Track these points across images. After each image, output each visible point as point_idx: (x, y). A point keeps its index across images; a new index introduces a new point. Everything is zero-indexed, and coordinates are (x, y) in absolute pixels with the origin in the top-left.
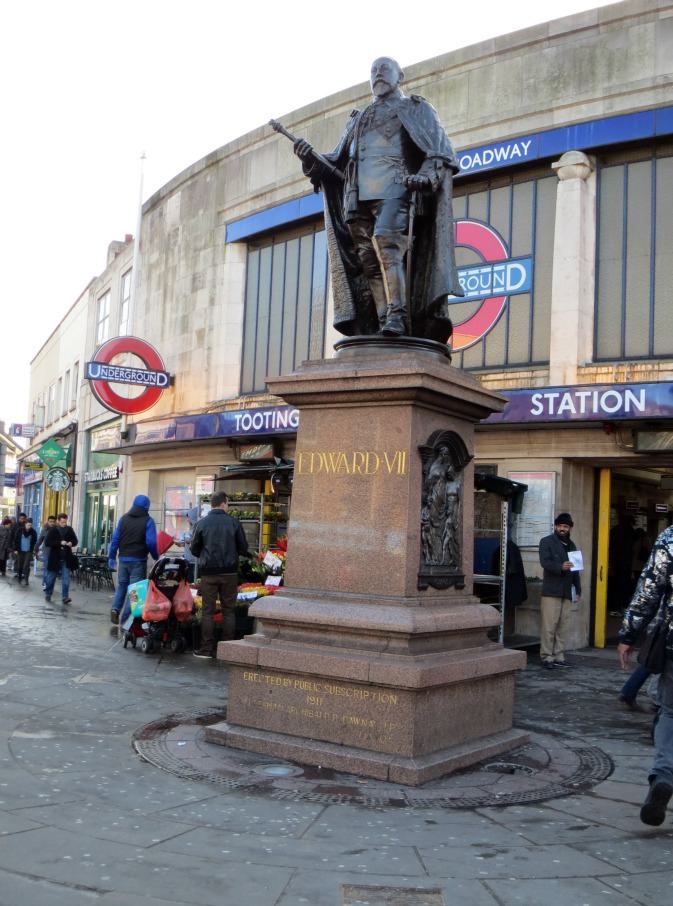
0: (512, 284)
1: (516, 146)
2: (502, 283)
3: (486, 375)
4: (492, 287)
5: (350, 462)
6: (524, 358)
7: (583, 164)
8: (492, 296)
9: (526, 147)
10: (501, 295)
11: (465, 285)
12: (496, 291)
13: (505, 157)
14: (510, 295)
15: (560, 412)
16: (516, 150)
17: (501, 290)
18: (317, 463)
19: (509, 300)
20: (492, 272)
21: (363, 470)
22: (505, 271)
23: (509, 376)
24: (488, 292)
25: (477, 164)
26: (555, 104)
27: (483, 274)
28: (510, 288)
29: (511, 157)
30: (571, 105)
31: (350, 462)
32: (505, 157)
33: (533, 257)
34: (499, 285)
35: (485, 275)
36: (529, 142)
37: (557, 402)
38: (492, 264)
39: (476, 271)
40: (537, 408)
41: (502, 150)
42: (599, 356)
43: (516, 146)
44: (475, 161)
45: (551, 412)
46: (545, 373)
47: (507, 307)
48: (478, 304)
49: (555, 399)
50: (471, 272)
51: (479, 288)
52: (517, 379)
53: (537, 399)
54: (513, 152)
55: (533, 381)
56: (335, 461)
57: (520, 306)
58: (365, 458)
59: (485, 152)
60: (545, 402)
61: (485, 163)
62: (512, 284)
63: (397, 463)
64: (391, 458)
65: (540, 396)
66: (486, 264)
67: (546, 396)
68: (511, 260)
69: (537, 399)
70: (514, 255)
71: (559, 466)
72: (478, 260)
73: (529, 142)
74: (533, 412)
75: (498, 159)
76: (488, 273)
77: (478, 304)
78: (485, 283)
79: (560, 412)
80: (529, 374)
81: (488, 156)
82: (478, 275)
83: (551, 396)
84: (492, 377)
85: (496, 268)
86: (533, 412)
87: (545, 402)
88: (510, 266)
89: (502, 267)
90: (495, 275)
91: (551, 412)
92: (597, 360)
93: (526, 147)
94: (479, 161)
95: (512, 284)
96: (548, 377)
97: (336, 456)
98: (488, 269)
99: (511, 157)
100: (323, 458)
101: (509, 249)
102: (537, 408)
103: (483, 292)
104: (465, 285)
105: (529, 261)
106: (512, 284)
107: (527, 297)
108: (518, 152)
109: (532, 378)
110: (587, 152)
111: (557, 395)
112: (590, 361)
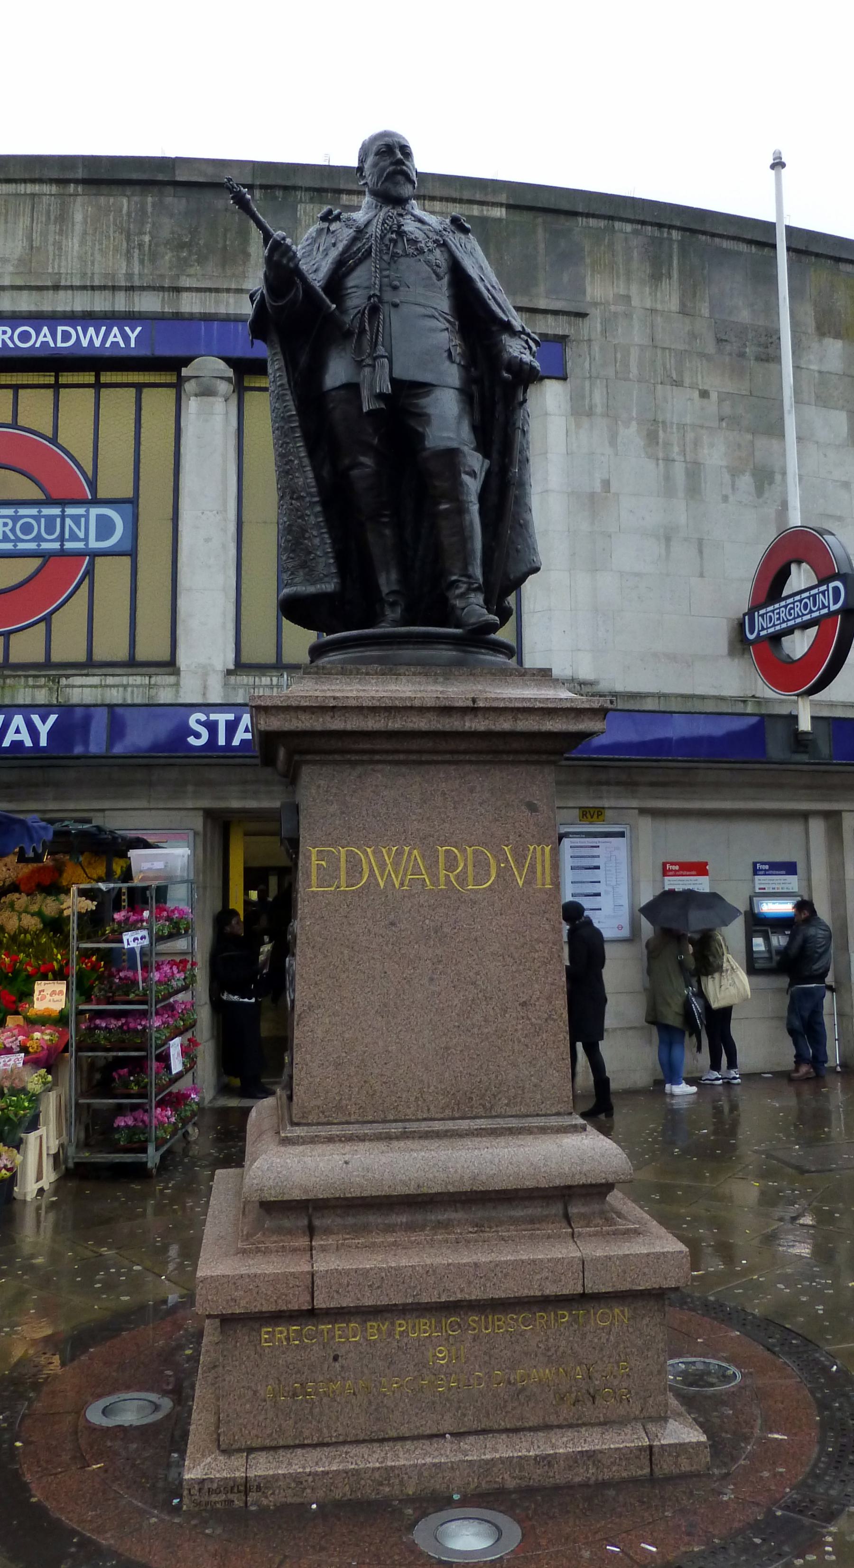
0: (100, 537)
1: (115, 330)
2: (81, 535)
3: (67, 677)
4: (61, 539)
5: (432, 866)
6: (122, 654)
7: (228, 380)
8: (62, 553)
9: (133, 336)
10: (79, 554)
11: (13, 530)
12: (68, 545)
13: (97, 344)
14: (95, 554)
15: (236, 742)
16: (115, 335)
17: (80, 545)
18: (354, 867)
19: (92, 564)
20: (63, 517)
21: (462, 879)
22: (87, 517)
23: (110, 680)
24: (56, 546)
25: (45, 344)
26: (185, 282)
27: (44, 516)
28: (94, 544)
29: (108, 345)
30: (210, 290)
31: (432, 866)
32: (97, 344)
33: (133, 501)
34: (74, 537)
35: (51, 519)
36: (139, 329)
37: (232, 727)
38: (62, 503)
39: (34, 511)
40: (198, 736)
41: (91, 331)
42: (244, 659)
43: (115, 330)
44: (41, 339)
45: (222, 741)
46: (172, 679)
47: (90, 573)
48: (37, 562)
49: (228, 723)
50: (22, 511)
51: (39, 538)
52: (125, 687)
53: (198, 722)
54: (111, 339)
55: (153, 692)
56: (396, 864)
57: (112, 576)
58: (465, 859)
59: (60, 329)
60: (212, 727)
61: (59, 344)
62: (99, 538)
63: (533, 867)
64: (520, 858)
65: (203, 718)
66: (50, 502)
67: (213, 717)
68: (96, 502)
69: (198, 722)
70: (101, 495)
71: (198, 822)
72: (41, 496)
73: (139, 329)
74: (192, 740)
75: (85, 343)
76: (54, 517)
77: (37, 562)
78: (50, 530)
79: (236, 742)
80: (146, 680)
81: (66, 336)
82: (37, 518)
83: (222, 718)
84: (78, 681)
85: (69, 511)
86: (192, 740)
87: (212, 727)
88: (94, 511)
89: (80, 511)
90: (68, 521)
91: (222, 741)
92: (241, 666)
93: (133, 336)
94: (49, 339)
95: (99, 538)
96: (177, 685)
97: (399, 853)
98: (56, 511)
99: (108, 345)
100: (367, 857)
101: (93, 484)
102: (198, 736)
103: (45, 546)
104: (13, 530)
105: (128, 507)
106: (100, 537)
107: (127, 560)
108: (119, 339)
109: (150, 686)
110: (228, 361)
111: (231, 717)
112: (232, 667)
